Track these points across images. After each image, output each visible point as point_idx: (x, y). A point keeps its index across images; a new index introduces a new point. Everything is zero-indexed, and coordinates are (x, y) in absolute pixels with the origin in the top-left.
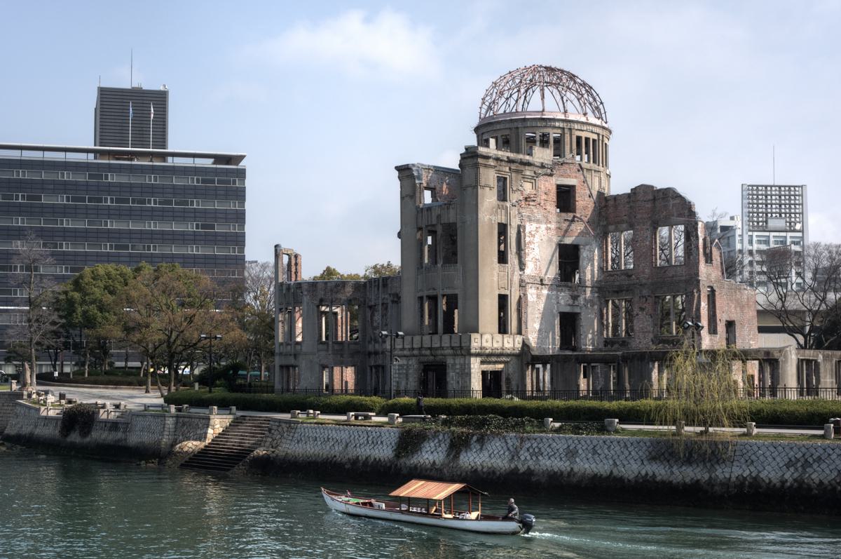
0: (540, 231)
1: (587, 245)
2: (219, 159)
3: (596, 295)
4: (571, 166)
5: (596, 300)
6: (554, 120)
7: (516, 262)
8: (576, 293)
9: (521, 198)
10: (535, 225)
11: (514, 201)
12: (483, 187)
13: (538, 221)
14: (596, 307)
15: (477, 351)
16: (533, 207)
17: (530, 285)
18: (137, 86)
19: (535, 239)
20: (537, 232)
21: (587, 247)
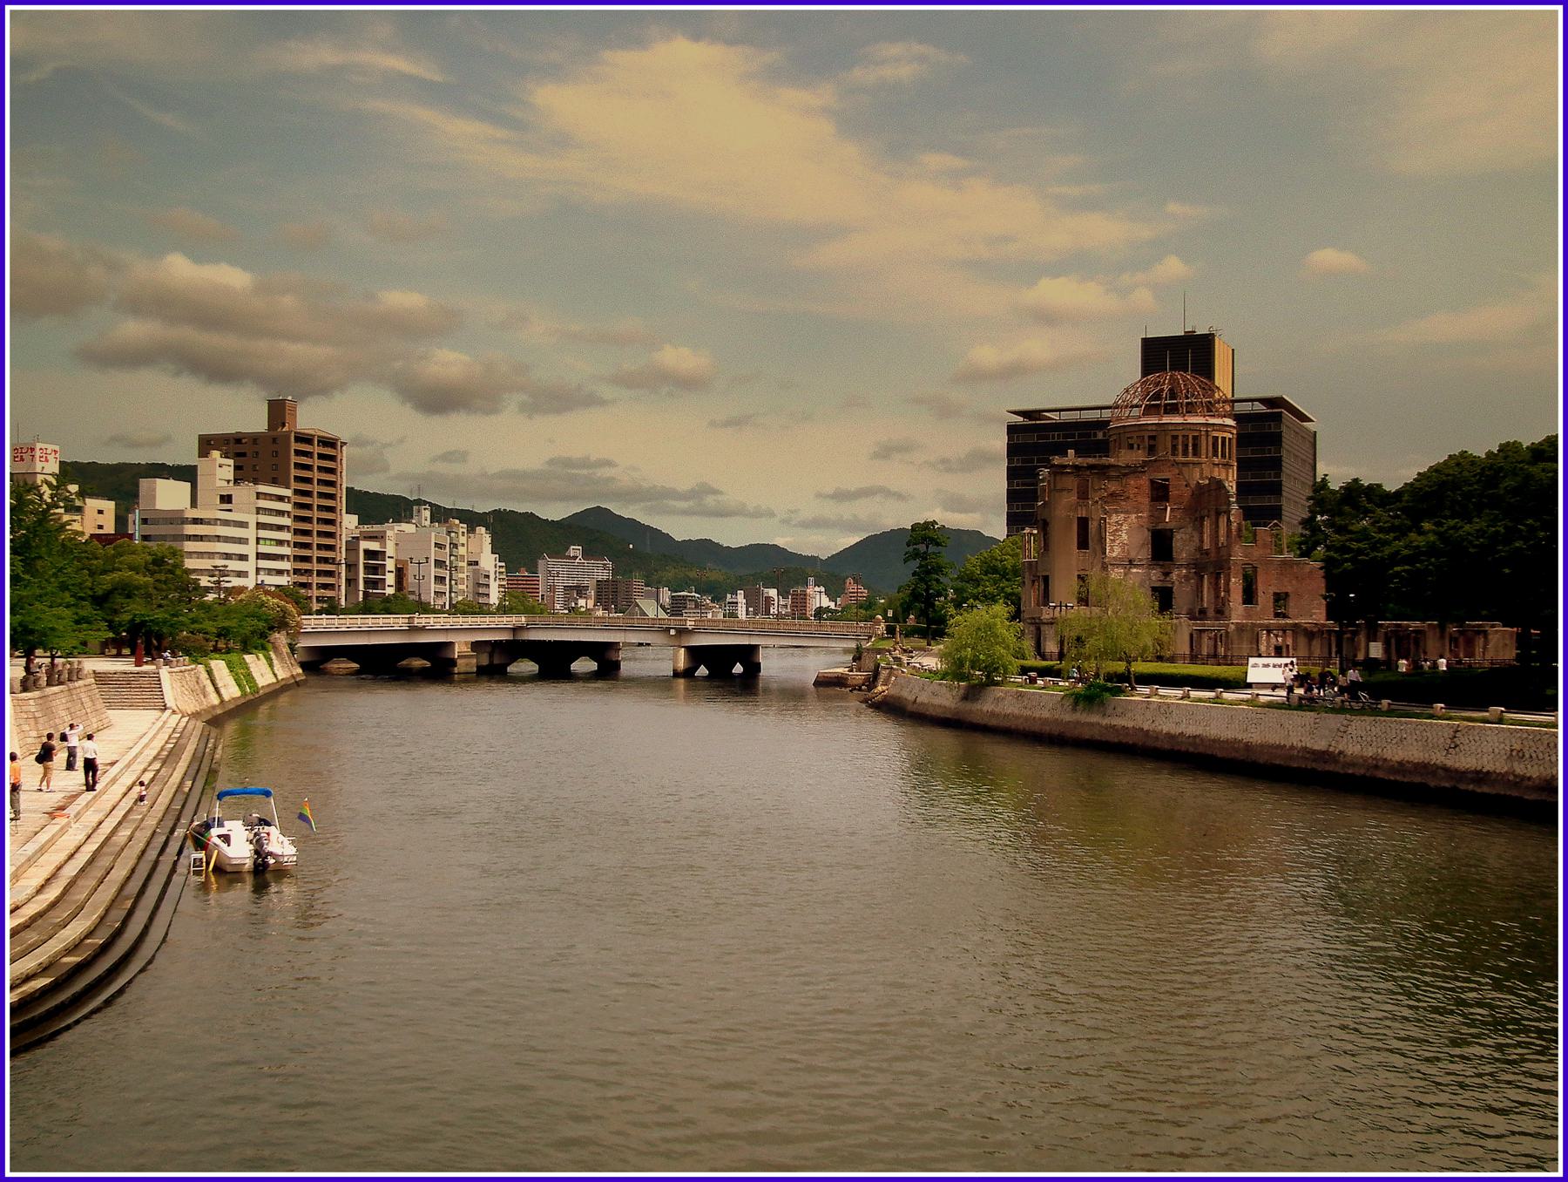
2: (1262, 401)
4: (1164, 462)
5: (1191, 575)
7: (1098, 548)
8: (1167, 570)
12: (1062, 490)
13: (1127, 512)
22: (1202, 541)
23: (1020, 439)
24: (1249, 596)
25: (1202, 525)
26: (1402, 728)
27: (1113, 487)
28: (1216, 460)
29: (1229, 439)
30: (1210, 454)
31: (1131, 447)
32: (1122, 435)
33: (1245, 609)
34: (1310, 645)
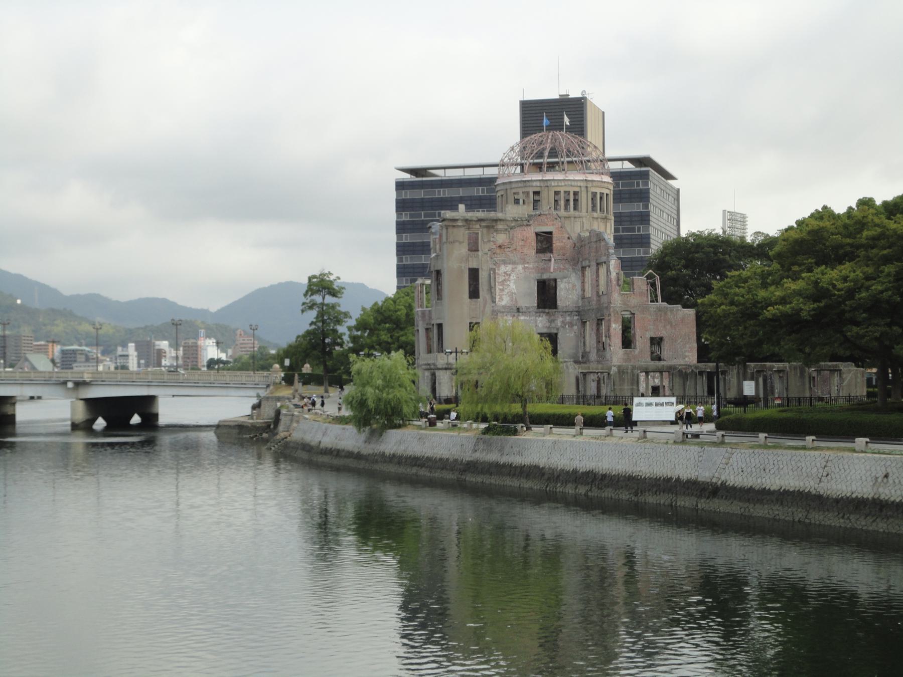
0: (517, 270)
1: (565, 278)
2: (632, 160)
3: (576, 318)
6: (531, 181)
7: (488, 297)
9: (494, 247)
10: (509, 268)
11: (487, 250)
13: (514, 263)
14: (575, 327)
15: (444, 366)
16: (508, 253)
17: (505, 314)
18: (564, 93)
19: (512, 277)
20: (513, 271)
21: (565, 280)
22: (583, 290)
23: (408, 195)
24: (627, 343)
25: (583, 275)
26: (779, 459)
27: (501, 238)
28: (595, 215)
29: (607, 194)
30: (590, 209)
31: (517, 201)
32: (508, 191)
33: (625, 353)
34: (684, 385)
